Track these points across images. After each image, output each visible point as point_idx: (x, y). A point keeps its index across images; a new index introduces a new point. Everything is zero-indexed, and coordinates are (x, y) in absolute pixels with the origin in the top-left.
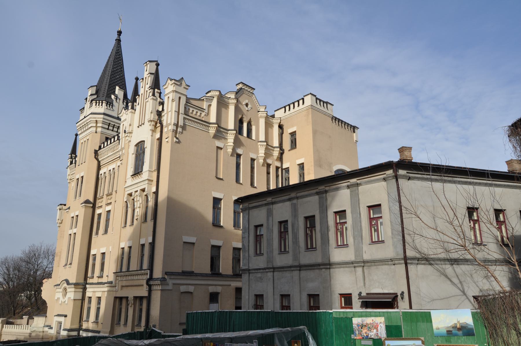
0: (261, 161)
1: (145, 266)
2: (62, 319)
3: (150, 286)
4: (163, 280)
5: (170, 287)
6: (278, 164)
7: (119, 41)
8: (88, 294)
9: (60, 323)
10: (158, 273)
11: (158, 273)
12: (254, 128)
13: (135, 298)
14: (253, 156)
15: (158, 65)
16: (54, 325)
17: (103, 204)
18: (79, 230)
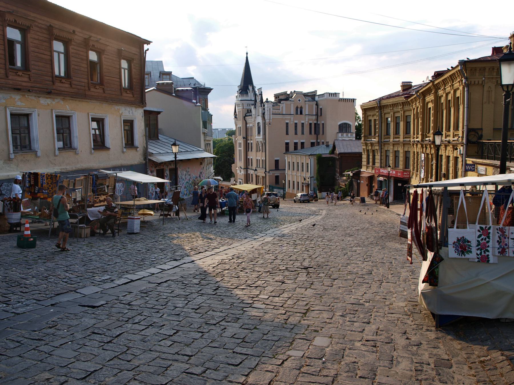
0: (307, 123)
1: (264, 167)
2: (241, 181)
3: (265, 174)
4: (269, 172)
5: (271, 174)
6: (315, 122)
7: (247, 58)
8: (249, 172)
9: (240, 182)
10: (267, 170)
11: (267, 170)
12: (303, 109)
13: (262, 177)
14: (303, 122)
15: (262, 92)
16: (238, 182)
17: (250, 139)
18: (242, 149)
